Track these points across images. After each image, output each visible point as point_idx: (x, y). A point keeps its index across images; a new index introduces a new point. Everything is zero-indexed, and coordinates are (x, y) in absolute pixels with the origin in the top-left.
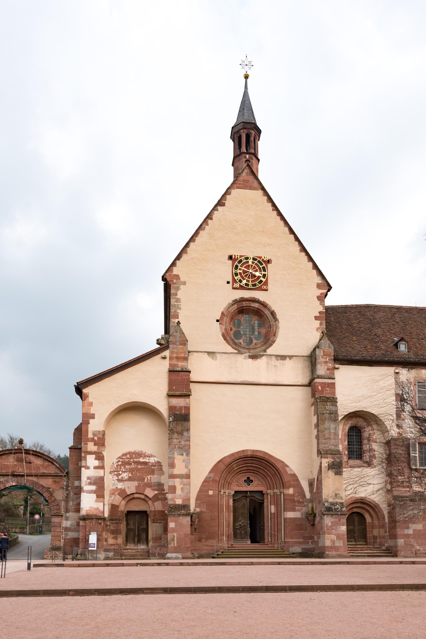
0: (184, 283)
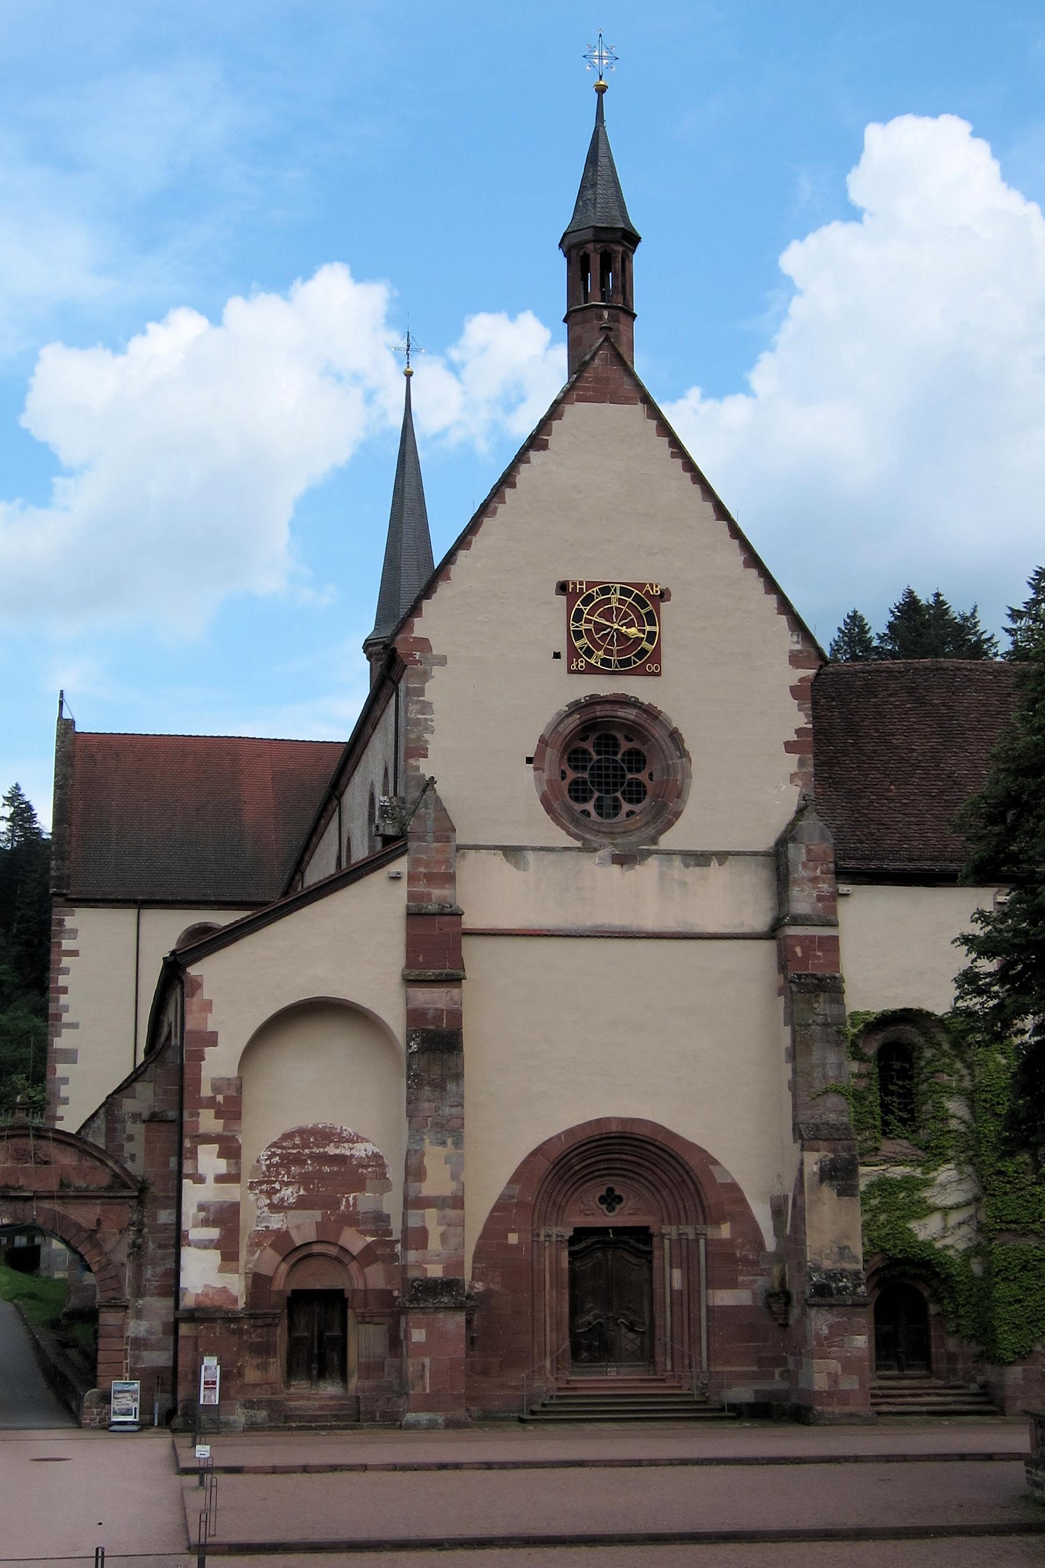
0: (442, 661)
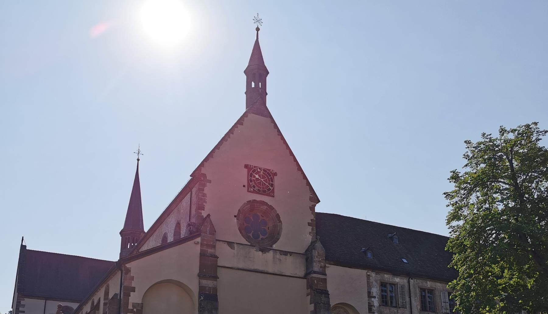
0: (210, 182)
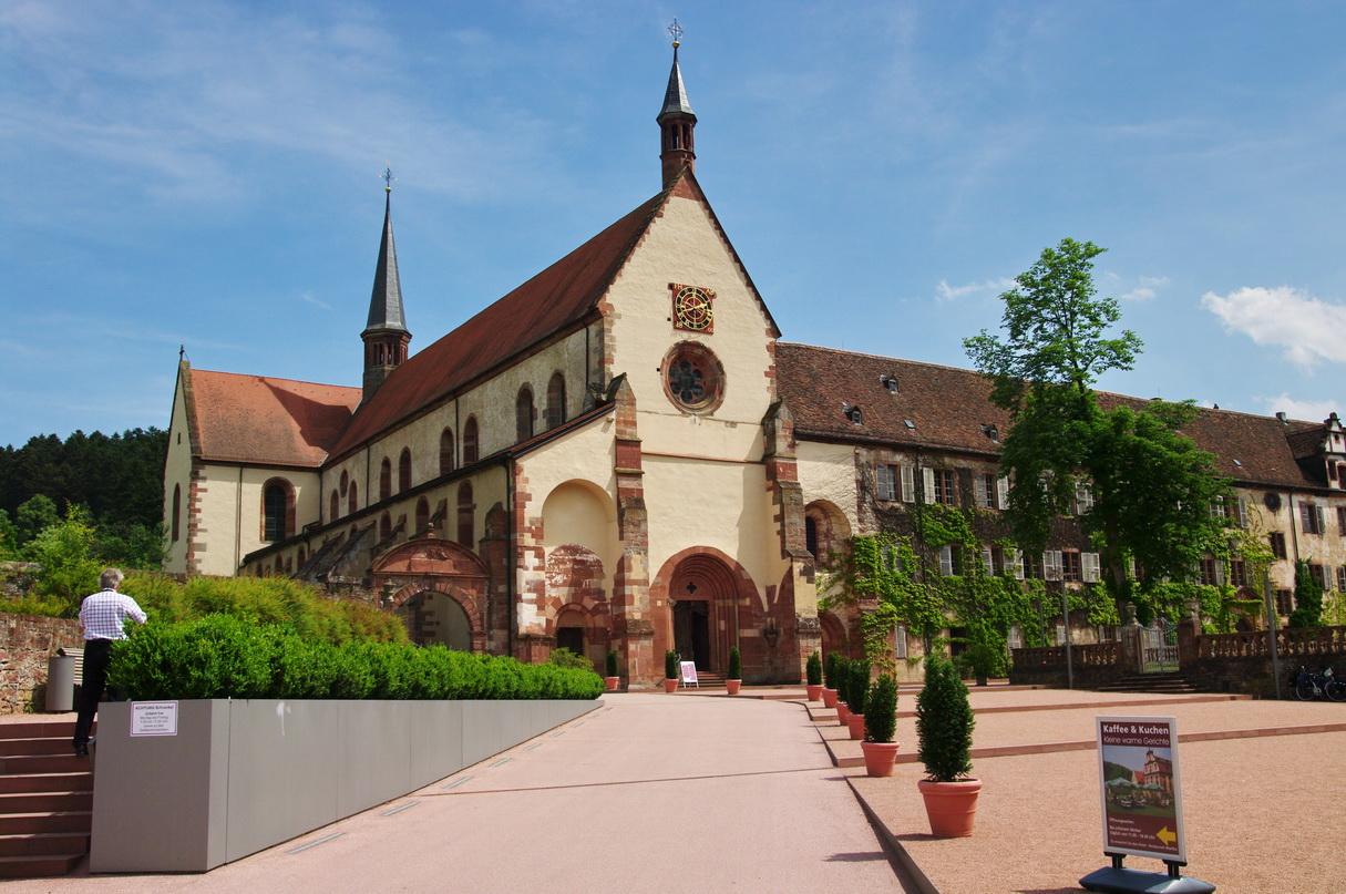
0: (619, 317)
